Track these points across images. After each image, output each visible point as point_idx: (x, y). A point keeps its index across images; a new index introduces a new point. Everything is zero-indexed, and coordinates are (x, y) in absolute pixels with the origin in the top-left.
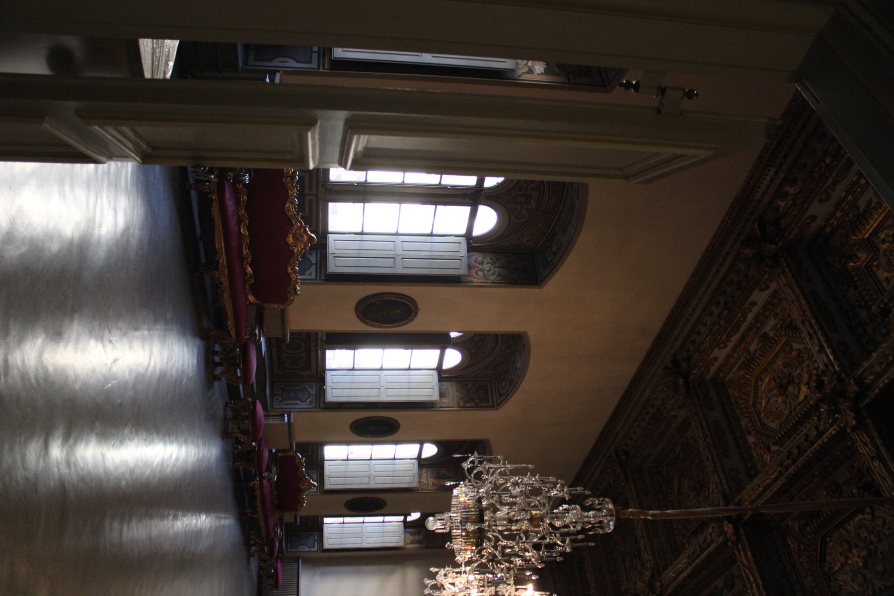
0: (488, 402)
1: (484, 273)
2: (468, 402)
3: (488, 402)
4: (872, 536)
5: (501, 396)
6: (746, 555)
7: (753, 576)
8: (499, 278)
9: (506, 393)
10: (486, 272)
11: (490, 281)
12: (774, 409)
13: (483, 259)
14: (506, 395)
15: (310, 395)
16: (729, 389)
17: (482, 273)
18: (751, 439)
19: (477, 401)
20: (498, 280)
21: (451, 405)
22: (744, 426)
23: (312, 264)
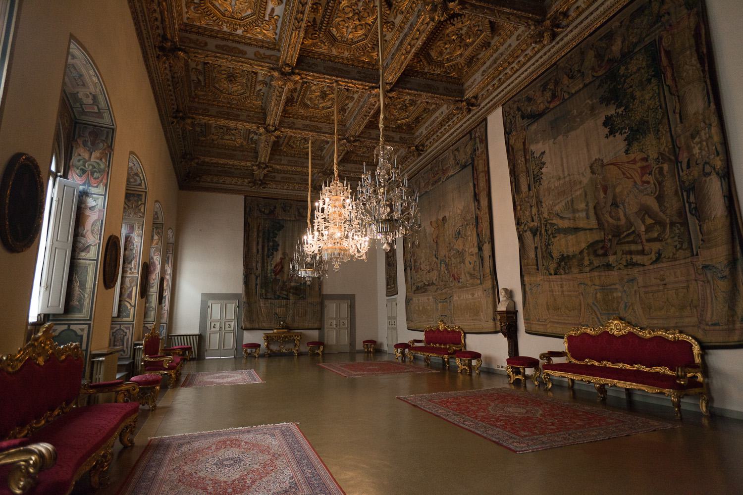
0: (141, 195)
1: (95, 171)
2: (140, 210)
3: (141, 195)
4: (353, 7)
5: (140, 185)
6: (309, 76)
7: (321, 78)
8: (104, 160)
9: (141, 180)
10: (95, 169)
11: (107, 169)
12: (241, 6)
13: (78, 169)
14: (143, 181)
15: (120, 329)
16: (195, 23)
17: (95, 174)
18: (240, 32)
19: (140, 203)
20: (106, 161)
21: (142, 223)
22: (229, 31)
23: (69, 329)
